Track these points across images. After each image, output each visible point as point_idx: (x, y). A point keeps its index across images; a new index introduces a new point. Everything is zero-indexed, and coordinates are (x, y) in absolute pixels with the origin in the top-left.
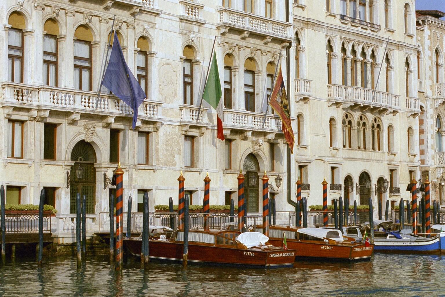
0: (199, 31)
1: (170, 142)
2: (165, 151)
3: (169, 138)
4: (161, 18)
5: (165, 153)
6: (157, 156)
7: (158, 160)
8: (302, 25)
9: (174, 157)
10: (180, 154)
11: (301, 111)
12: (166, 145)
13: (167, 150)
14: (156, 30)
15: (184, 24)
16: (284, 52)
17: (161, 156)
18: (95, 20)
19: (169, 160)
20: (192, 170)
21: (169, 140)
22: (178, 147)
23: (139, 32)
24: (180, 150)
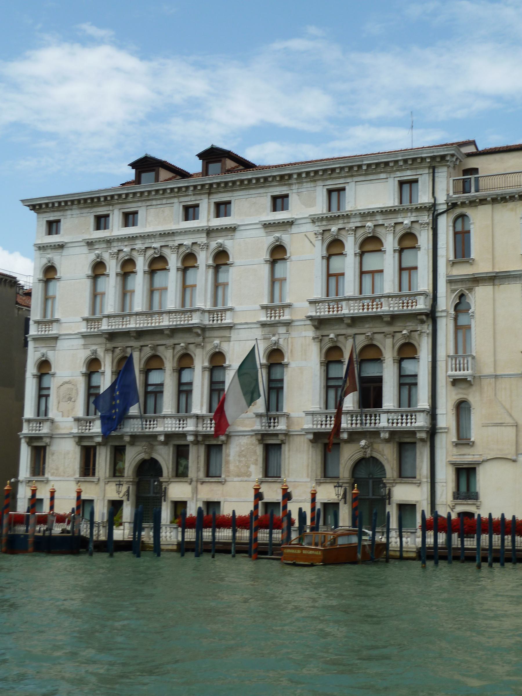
0: (287, 331)
1: (243, 453)
2: (237, 462)
3: (243, 449)
4: (237, 329)
5: (237, 464)
6: (228, 467)
7: (229, 472)
8: (469, 285)
9: (248, 467)
10: (256, 464)
11: (465, 396)
12: (239, 456)
13: (240, 461)
14: (232, 343)
15: (267, 329)
16: (427, 328)
17: (232, 467)
18: (192, 347)
19: (242, 470)
20: (270, 481)
21: (243, 451)
22: (254, 458)
23: (209, 348)
24: (257, 460)
